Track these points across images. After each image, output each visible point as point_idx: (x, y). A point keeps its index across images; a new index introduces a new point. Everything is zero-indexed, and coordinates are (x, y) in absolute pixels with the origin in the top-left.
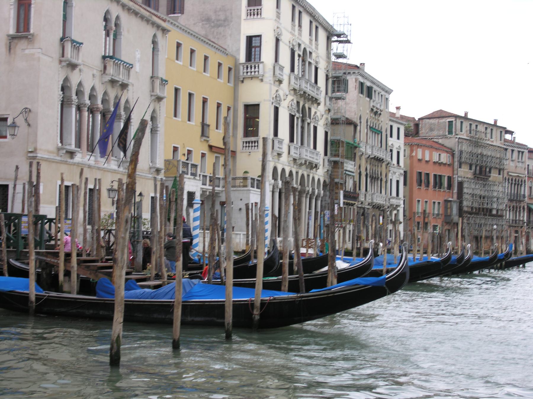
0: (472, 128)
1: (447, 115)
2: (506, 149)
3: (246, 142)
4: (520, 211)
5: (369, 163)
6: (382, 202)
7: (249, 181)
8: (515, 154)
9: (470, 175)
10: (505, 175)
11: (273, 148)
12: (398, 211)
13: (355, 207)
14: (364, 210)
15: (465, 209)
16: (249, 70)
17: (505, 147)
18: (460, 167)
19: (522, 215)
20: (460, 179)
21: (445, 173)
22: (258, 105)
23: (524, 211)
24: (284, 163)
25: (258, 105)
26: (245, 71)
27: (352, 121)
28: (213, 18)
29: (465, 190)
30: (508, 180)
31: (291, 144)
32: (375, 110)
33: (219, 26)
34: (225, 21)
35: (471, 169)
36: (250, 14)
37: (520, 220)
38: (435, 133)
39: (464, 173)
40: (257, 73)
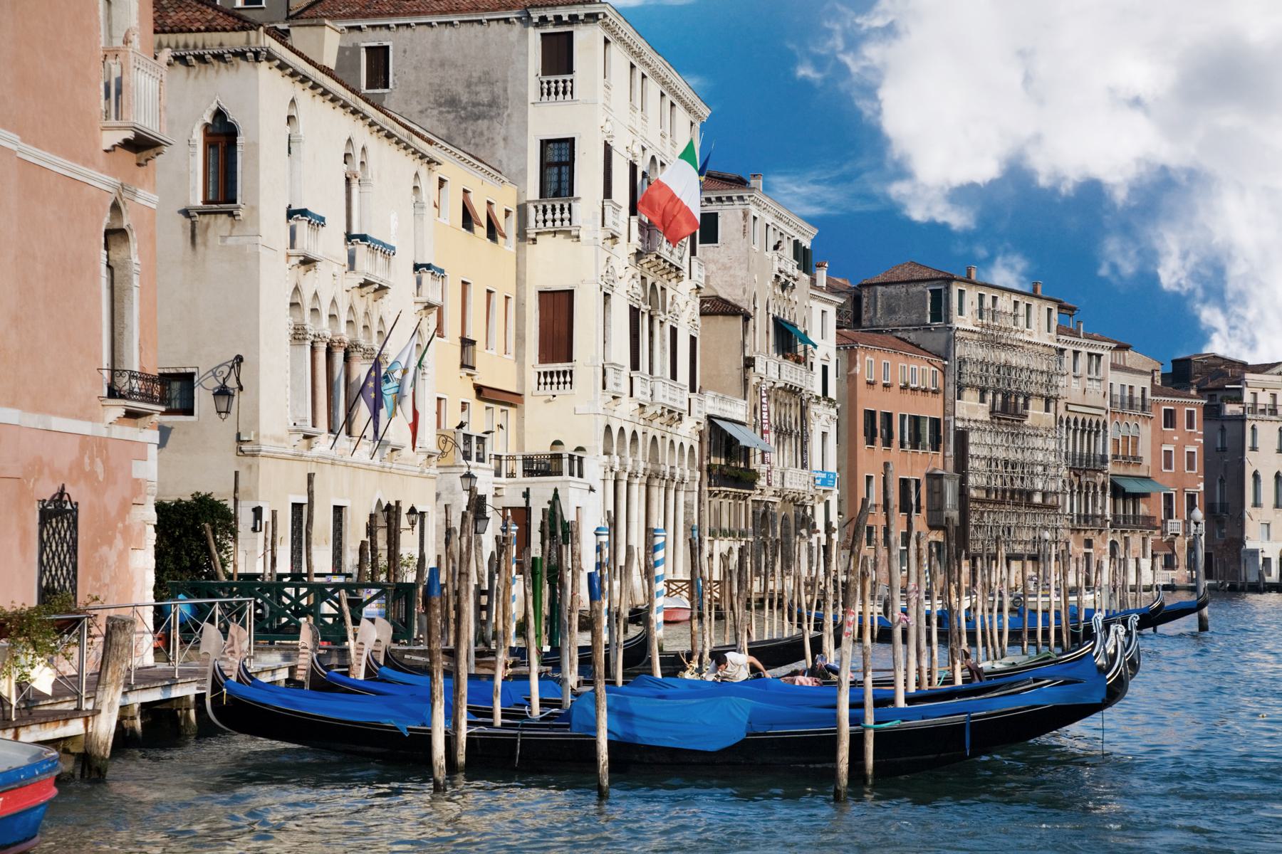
0: (985, 306)
1: (927, 275)
2: (1062, 351)
3: (545, 373)
4: (1095, 492)
5: (772, 399)
6: (801, 488)
7: (566, 462)
8: (1083, 361)
9: (983, 413)
10: (1061, 411)
11: (604, 387)
12: (827, 503)
13: (750, 503)
14: (767, 507)
15: (974, 493)
16: (549, 215)
17: (1060, 346)
18: (959, 398)
19: (1100, 504)
20: (959, 424)
21: (930, 408)
22: (570, 293)
23: (1104, 493)
24: (625, 415)
25: (570, 293)
26: (540, 217)
27: (740, 308)
28: (465, 98)
29: (972, 450)
30: (1068, 422)
31: (634, 374)
32: (783, 277)
33: (478, 117)
34: (490, 105)
35: (982, 400)
36: (547, 92)
37: (1095, 516)
38: (901, 317)
39: (972, 409)
40: (566, 223)
